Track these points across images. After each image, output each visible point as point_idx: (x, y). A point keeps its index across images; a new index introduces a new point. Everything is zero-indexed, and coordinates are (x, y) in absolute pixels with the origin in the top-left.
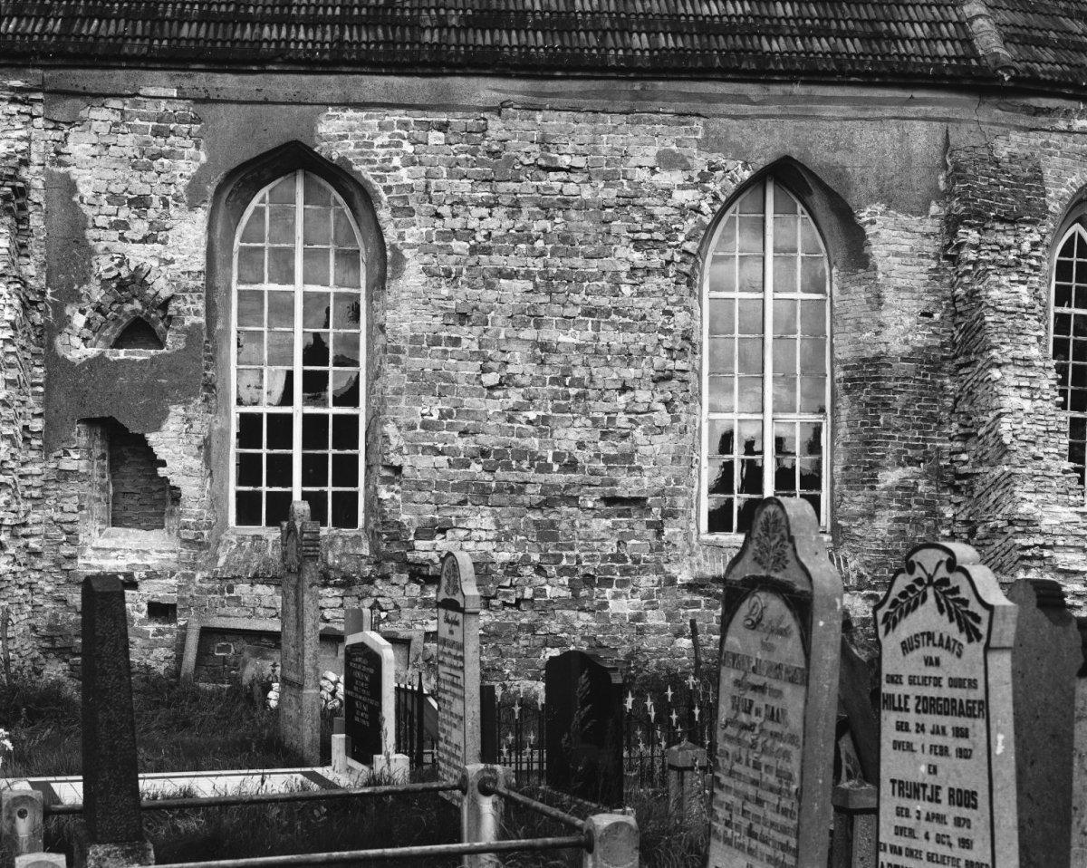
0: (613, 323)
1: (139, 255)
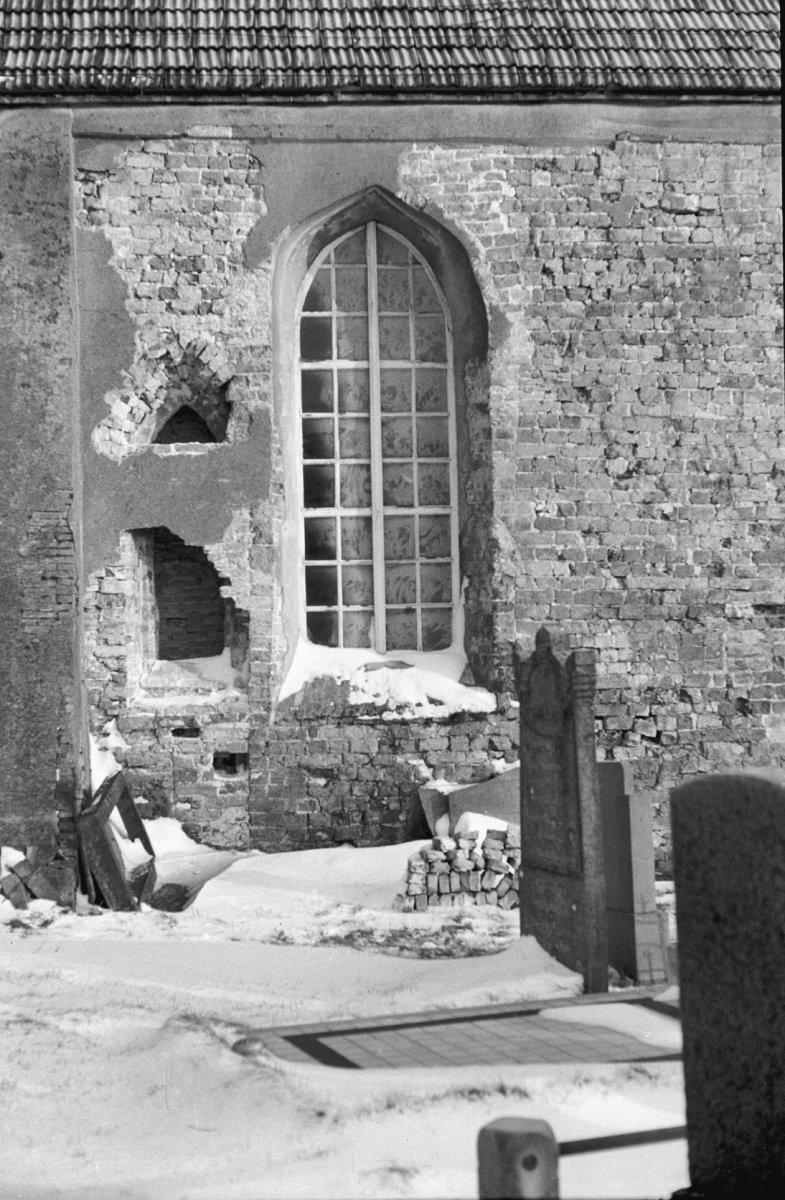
0: (758, 393)
1: (194, 330)
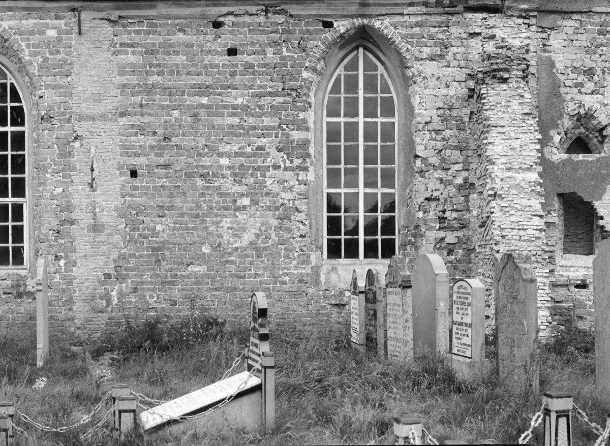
1: (590, 101)
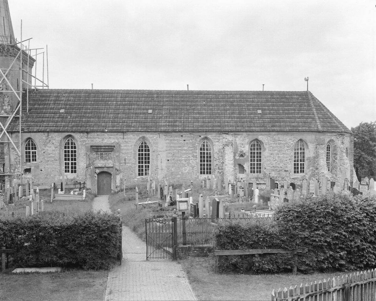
1: (243, 149)
